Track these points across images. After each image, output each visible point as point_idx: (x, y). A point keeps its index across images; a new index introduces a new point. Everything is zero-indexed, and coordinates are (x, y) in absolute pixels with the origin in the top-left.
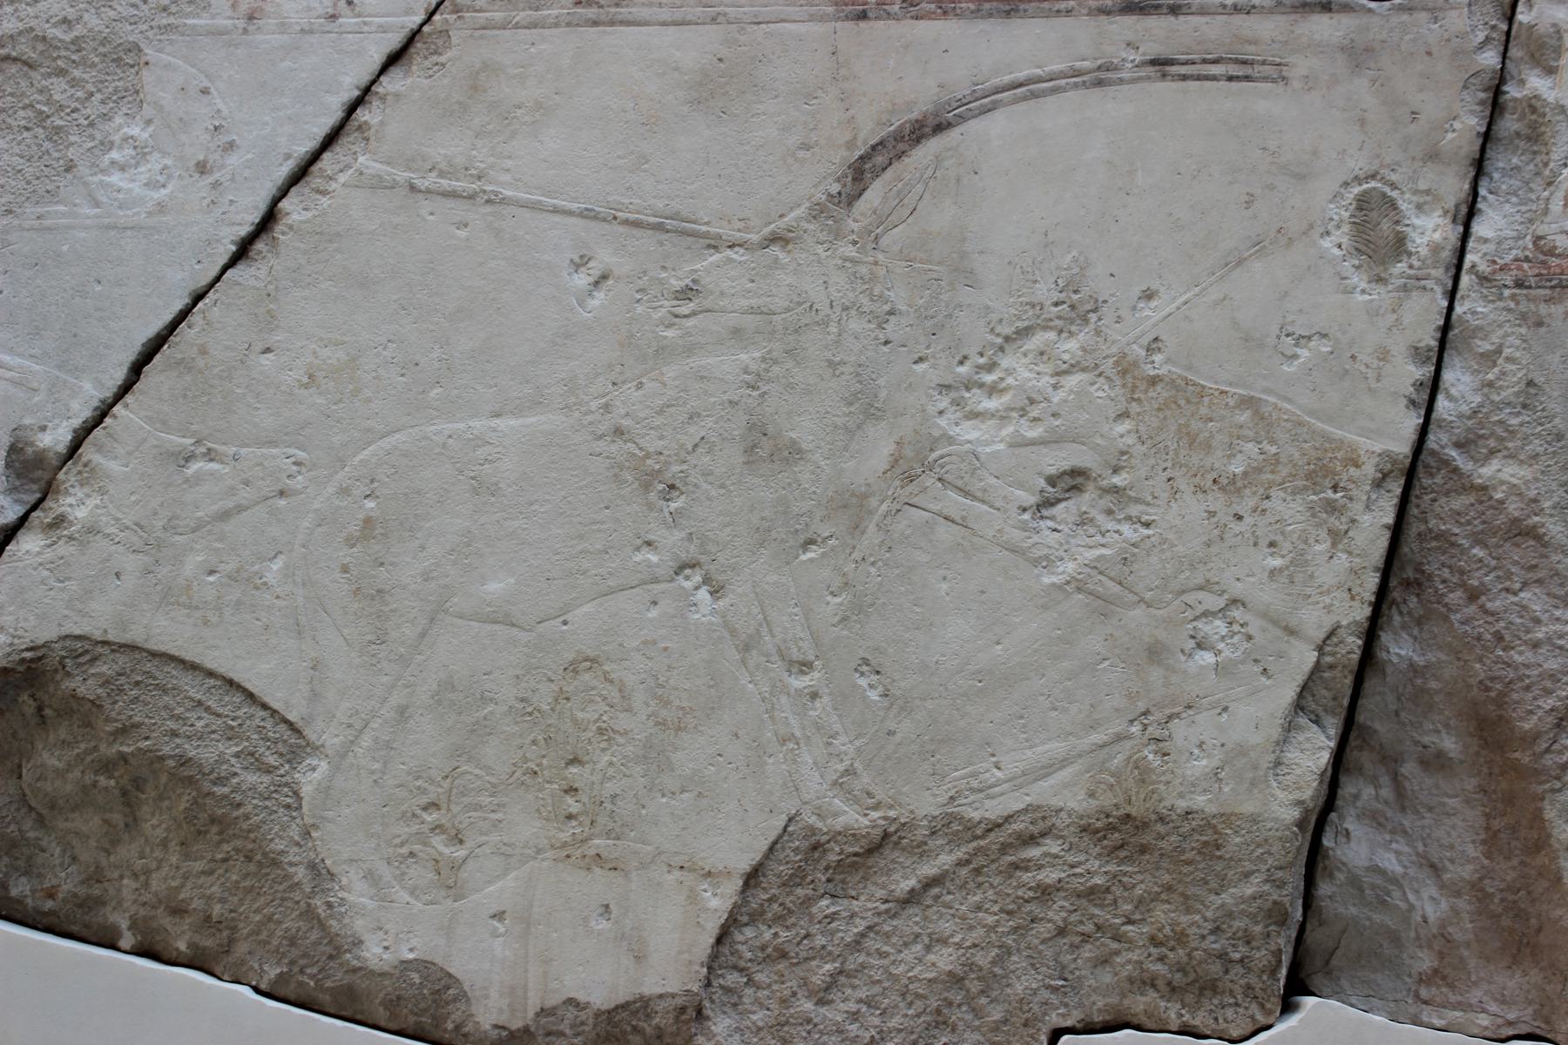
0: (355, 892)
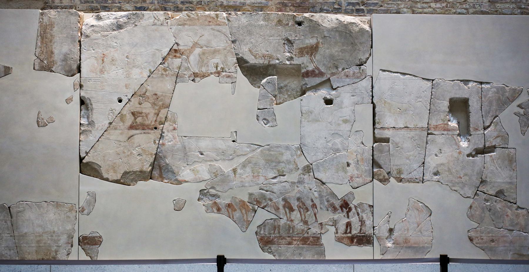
0: (104, 174)
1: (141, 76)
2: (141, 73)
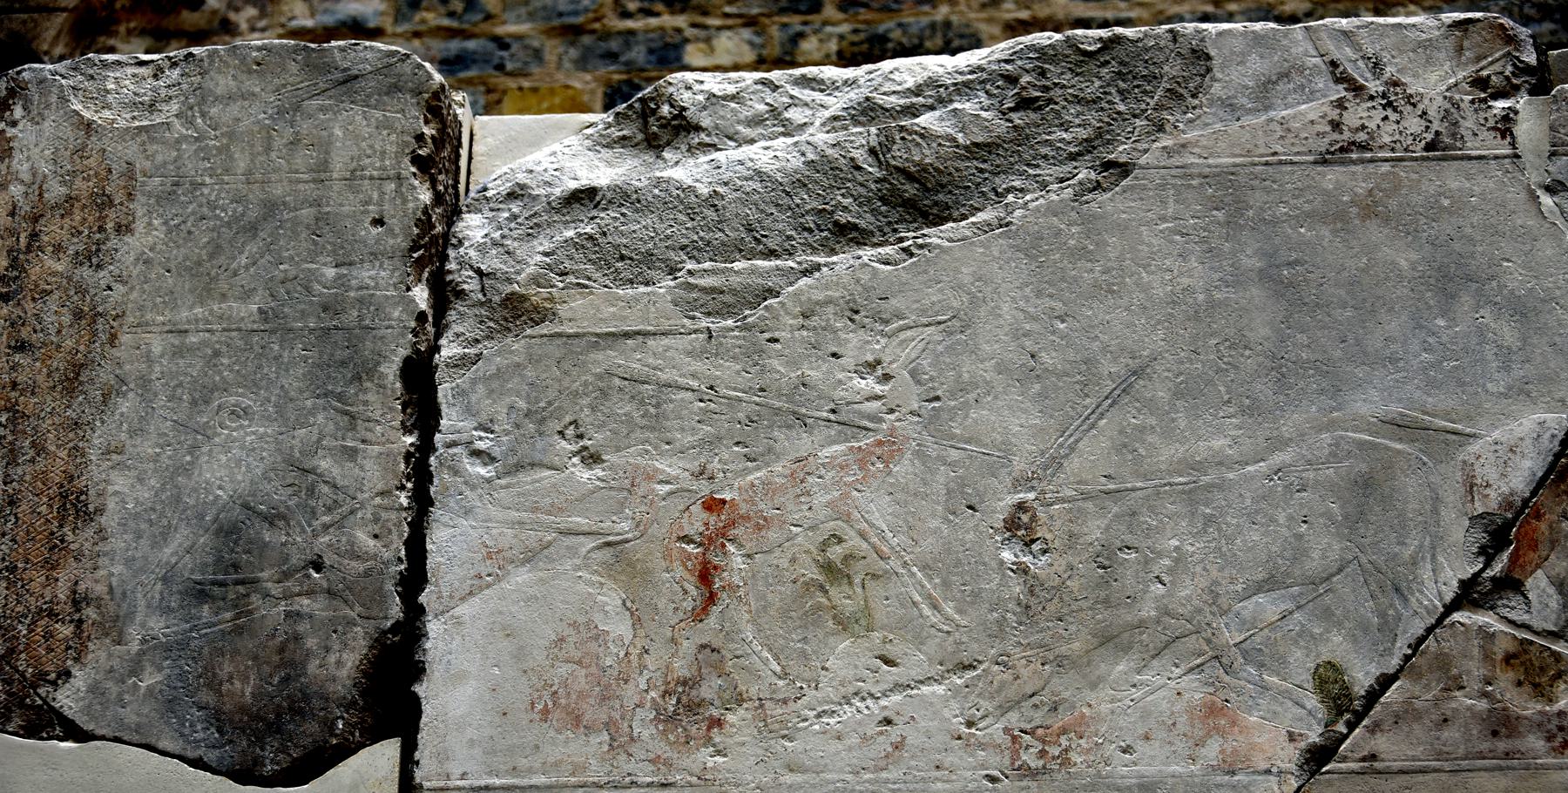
1: (1212, 751)
2: (1214, 714)
